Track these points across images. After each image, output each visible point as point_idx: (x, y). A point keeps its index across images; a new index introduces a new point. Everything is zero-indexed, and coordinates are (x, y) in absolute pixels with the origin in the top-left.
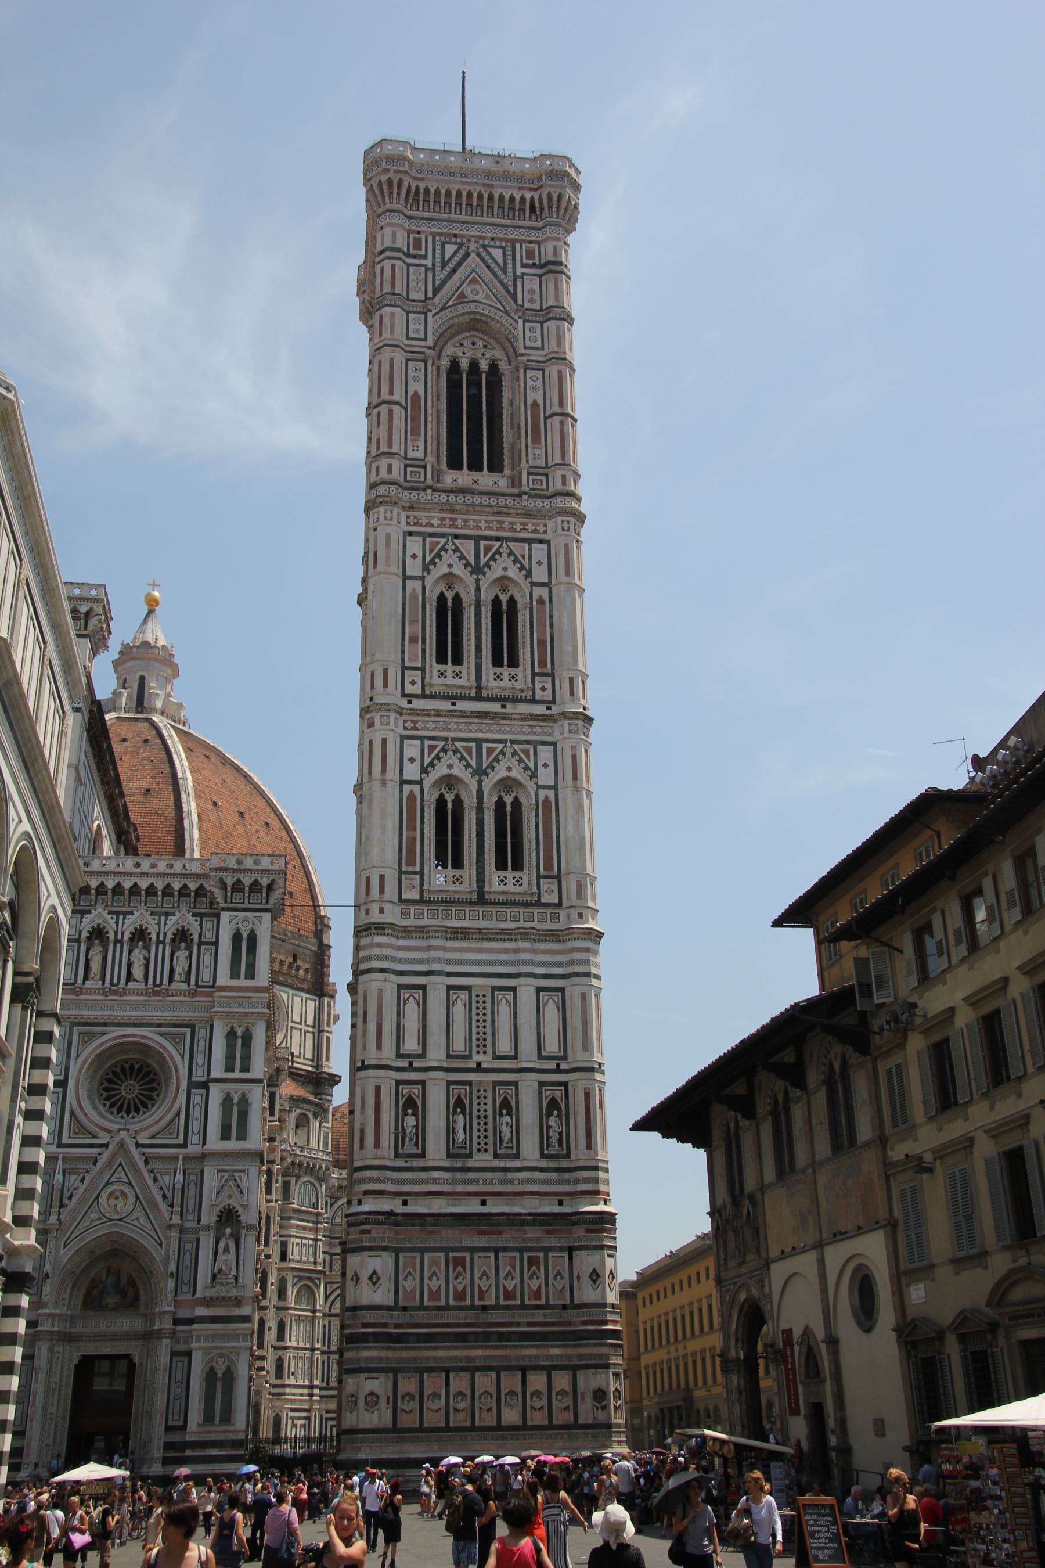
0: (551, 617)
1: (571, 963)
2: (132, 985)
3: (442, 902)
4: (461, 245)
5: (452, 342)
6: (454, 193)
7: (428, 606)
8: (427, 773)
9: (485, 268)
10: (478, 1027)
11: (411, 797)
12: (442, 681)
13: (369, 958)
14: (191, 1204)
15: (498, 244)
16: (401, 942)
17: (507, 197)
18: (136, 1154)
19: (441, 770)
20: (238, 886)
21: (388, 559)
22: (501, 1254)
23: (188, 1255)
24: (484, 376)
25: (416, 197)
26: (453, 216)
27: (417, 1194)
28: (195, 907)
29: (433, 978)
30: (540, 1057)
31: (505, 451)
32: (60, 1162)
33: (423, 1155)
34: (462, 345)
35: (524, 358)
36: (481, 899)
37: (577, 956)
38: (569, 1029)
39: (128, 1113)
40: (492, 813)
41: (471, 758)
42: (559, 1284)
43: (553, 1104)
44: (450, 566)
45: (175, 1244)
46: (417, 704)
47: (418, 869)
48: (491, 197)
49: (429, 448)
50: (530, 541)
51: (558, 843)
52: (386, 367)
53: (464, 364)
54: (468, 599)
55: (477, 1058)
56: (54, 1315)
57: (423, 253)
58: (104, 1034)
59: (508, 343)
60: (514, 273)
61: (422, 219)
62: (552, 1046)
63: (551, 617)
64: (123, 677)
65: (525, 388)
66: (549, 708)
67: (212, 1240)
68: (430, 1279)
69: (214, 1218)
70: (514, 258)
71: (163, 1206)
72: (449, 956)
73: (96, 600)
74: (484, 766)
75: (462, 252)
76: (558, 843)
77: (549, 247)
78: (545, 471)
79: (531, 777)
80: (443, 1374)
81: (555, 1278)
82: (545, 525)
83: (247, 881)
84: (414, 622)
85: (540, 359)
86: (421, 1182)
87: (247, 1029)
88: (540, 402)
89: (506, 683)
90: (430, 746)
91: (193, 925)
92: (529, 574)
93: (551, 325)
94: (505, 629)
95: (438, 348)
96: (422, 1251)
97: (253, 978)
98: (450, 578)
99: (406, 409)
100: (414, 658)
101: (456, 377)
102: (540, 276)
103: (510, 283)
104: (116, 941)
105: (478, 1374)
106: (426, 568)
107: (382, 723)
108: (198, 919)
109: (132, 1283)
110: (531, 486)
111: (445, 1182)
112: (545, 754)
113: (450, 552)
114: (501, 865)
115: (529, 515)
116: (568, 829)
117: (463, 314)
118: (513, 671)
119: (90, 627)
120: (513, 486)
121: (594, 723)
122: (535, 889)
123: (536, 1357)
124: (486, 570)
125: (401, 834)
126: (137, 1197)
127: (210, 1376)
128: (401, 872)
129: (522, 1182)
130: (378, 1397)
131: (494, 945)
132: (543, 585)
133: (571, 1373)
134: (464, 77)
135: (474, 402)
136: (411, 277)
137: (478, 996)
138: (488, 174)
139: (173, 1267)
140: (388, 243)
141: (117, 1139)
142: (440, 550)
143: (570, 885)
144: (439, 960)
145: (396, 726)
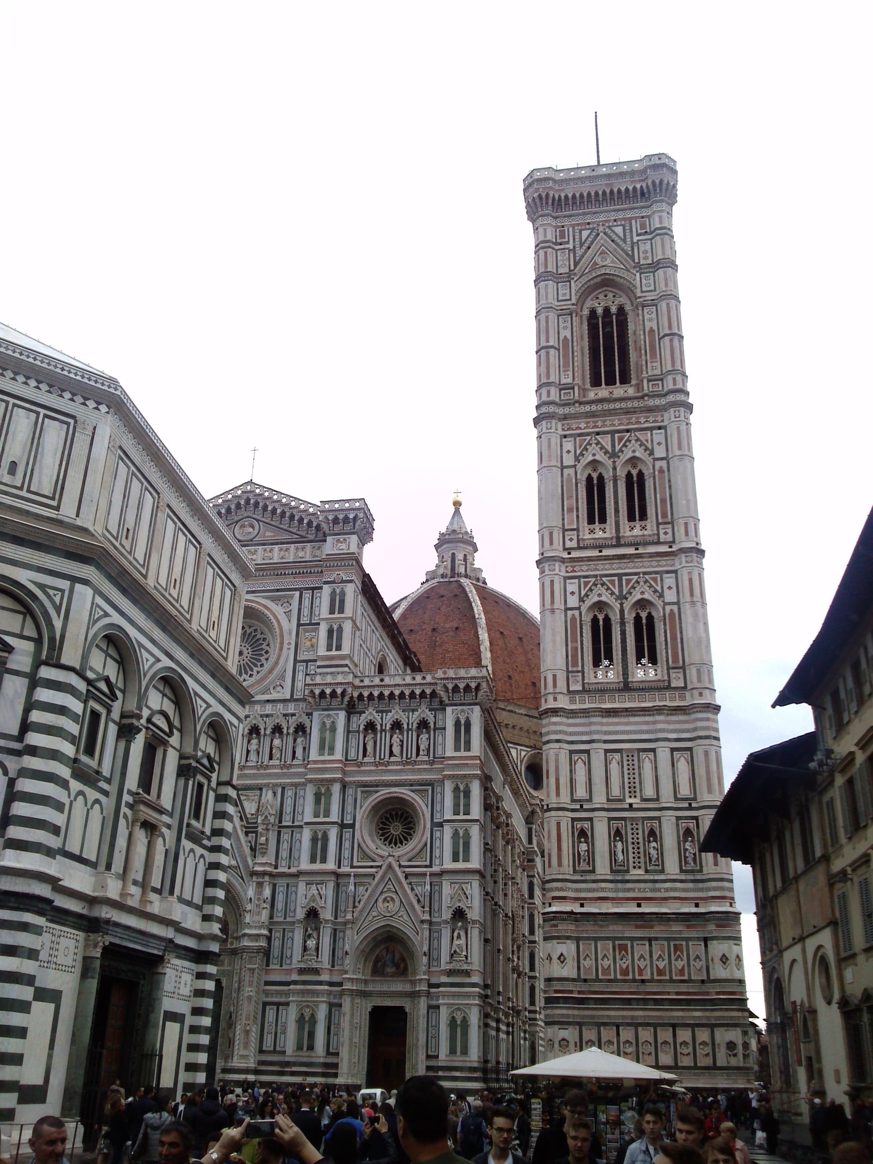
0: (669, 481)
1: (695, 729)
2: (393, 759)
5: (590, 298)
6: (585, 194)
8: (584, 601)
11: (573, 618)
13: (548, 733)
14: (436, 906)
15: (619, 223)
16: (571, 721)
17: (623, 189)
18: (399, 872)
20: (456, 689)
21: (550, 456)
22: (653, 943)
23: (436, 941)
24: (614, 317)
27: (590, 899)
29: (594, 745)
30: (676, 799)
31: (632, 368)
32: (352, 878)
33: (593, 871)
34: (597, 298)
36: (626, 687)
37: (699, 724)
39: (396, 844)
40: (632, 626)
41: (615, 588)
42: (698, 964)
43: (688, 832)
44: (594, 455)
45: (427, 933)
46: (575, 554)
47: (580, 669)
48: (612, 192)
49: (576, 374)
50: (651, 429)
52: (543, 323)
53: (600, 311)
54: (608, 475)
56: (353, 979)
58: (377, 792)
59: (629, 291)
60: (632, 241)
61: (565, 217)
62: (685, 790)
63: (669, 481)
66: (671, 547)
67: (449, 931)
68: (602, 959)
69: (450, 916)
71: (417, 907)
72: (605, 728)
73: (358, 509)
74: (624, 593)
76: (682, 643)
77: (656, 218)
79: (659, 597)
80: (615, 1028)
81: (695, 960)
82: (662, 416)
83: (462, 686)
86: (593, 890)
87: (467, 785)
88: (655, 328)
89: (637, 532)
90: (585, 582)
91: (430, 717)
92: (652, 453)
93: (661, 272)
95: (579, 304)
96: (596, 939)
97: (469, 750)
98: (594, 463)
99: (559, 350)
100: (572, 523)
101: (595, 321)
102: (651, 239)
104: (382, 730)
105: (640, 1029)
106: (577, 459)
107: (550, 570)
109: (403, 959)
111: (610, 890)
112: (669, 580)
113: (594, 445)
115: (650, 410)
116: (689, 632)
119: (357, 526)
120: (638, 392)
121: (706, 554)
122: (666, 678)
123: (682, 1017)
124: (620, 454)
126: (401, 901)
127: (453, 1023)
128: (568, 672)
129: (667, 890)
130: (568, 1042)
131: (637, 719)
132: (662, 459)
133: (709, 1030)
135: (608, 336)
138: (609, 176)
139: (426, 949)
140: (541, 238)
141: (387, 862)
143: (692, 673)
144: (597, 732)
145: (560, 571)
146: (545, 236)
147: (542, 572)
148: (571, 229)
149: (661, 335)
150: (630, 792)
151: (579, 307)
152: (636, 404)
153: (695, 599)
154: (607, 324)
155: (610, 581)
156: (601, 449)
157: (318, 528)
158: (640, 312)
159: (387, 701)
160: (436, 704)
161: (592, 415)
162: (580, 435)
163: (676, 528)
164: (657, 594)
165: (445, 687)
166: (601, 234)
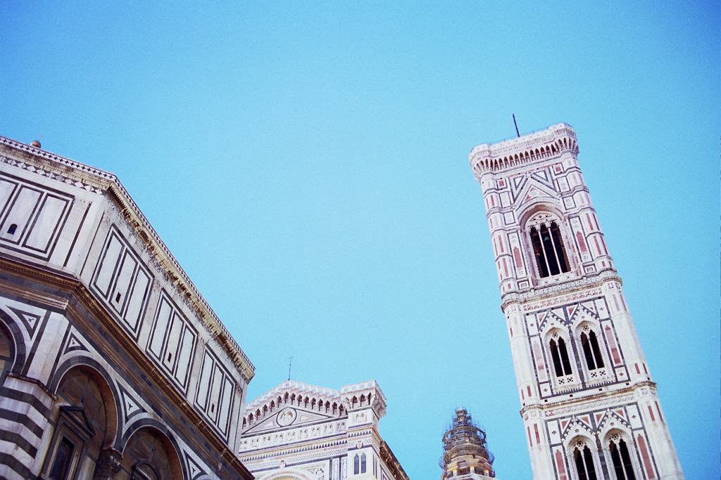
0: (616, 334)
4: (523, 177)
5: (529, 219)
7: (545, 348)
8: (564, 438)
11: (558, 453)
24: (549, 229)
25: (495, 165)
26: (516, 166)
35: (567, 214)
40: (609, 453)
46: (550, 401)
49: (528, 270)
50: (593, 300)
53: (538, 227)
63: (616, 334)
65: (571, 228)
70: (550, 173)
75: (524, 179)
78: (593, 263)
79: (627, 425)
84: (538, 359)
88: (581, 231)
92: (597, 316)
101: (535, 235)
106: (539, 329)
112: (632, 410)
113: (551, 317)
115: (590, 286)
119: (371, 403)
125: (556, 476)
132: (607, 319)
135: (548, 244)
145: (540, 416)
146: (489, 185)
148: (507, 179)
154: (545, 234)
155: (584, 419)
156: (557, 319)
157: (341, 408)
162: (538, 312)
164: (625, 423)
166: (530, 179)
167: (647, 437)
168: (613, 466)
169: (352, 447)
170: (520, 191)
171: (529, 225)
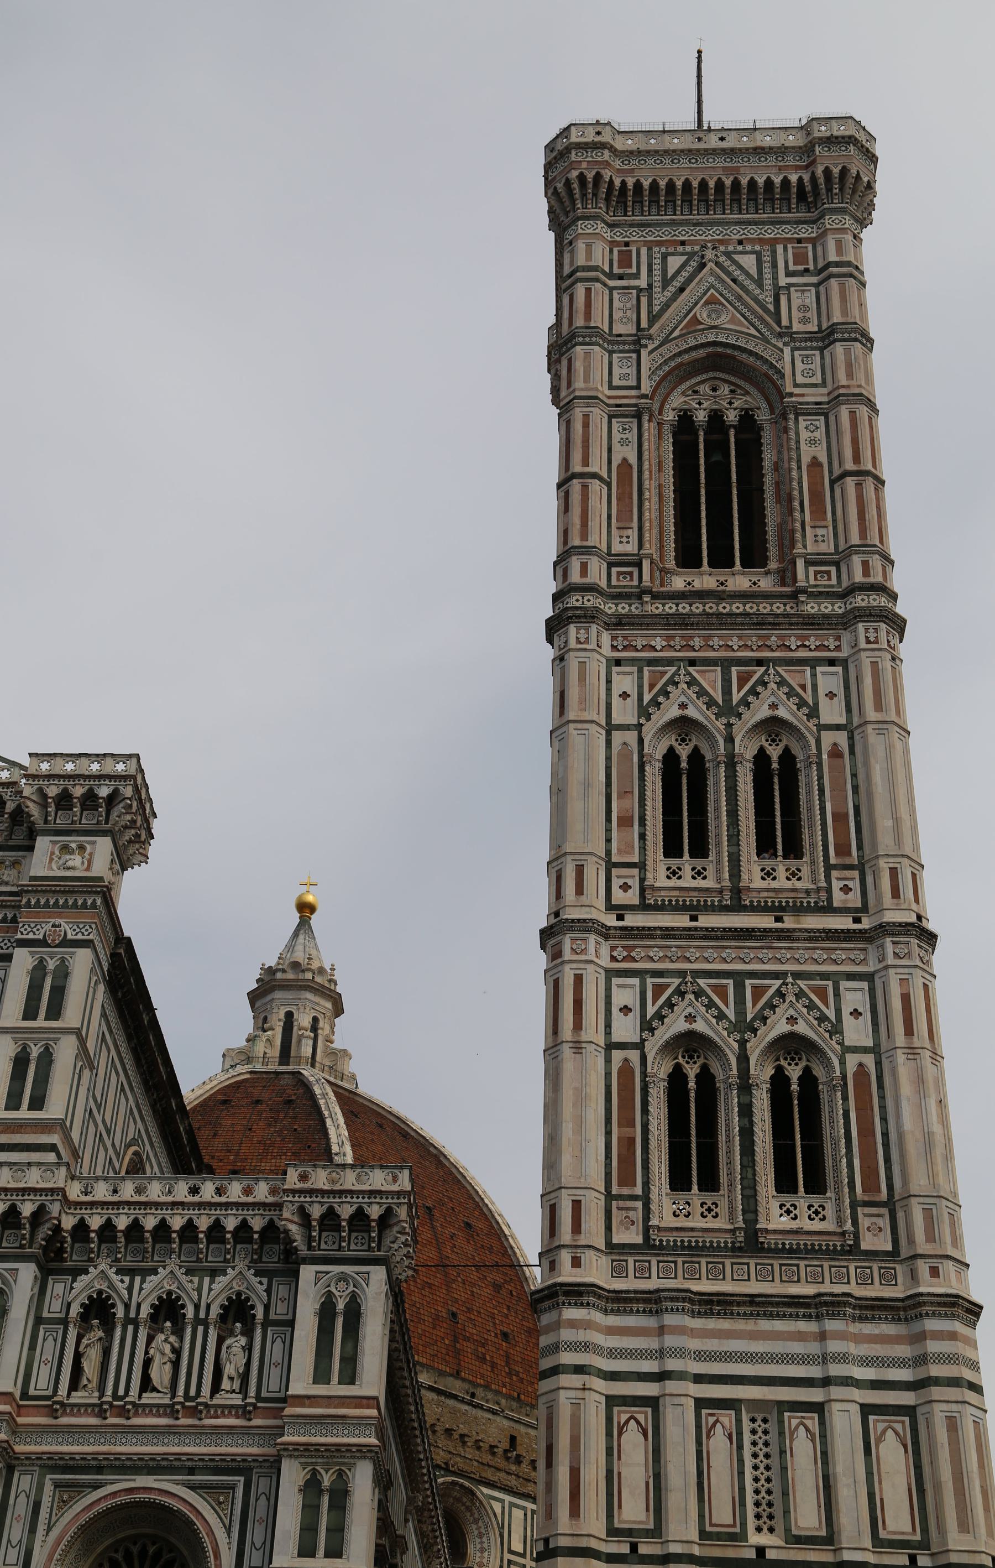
3: (683, 1247)
5: (679, 390)
6: (679, 184)
7: (647, 768)
8: (652, 1030)
9: (728, 281)
10: (756, 1480)
11: (626, 1069)
12: (673, 883)
15: (749, 248)
16: (613, 1320)
17: (761, 181)
19: (676, 1025)
21: (583, 701)
24: (732, 432)
28: (260, 1260)
34: (696, 392)
38: (928, 1486)
44: (683, 706)
46: (631, 920)
47: (638, 1190)
48: (736, 184)
51: (886, 1145)
53: (701, 416)
54: (715, 752)
55: (755, 1539)
57: (634, 270)
63: (854, 775)
64: (262, 1016)
65: (798, 442)
66: (857, 920)
70: (774, 265)
74: (749, 1019)
75: (694, 264)
76: (886, 1145)
79: (831, 1034)
82: (838, 638)
83: (346, 1211)
84: (625, 793)
85: (819, 399)
88: (823, 459)
89: (782, 882)
90: (655, 986)
92: (814, 712)
93: (839, 348)
94: (777, 800)
95: (658, 399)
99: (609, 485)
100: (628, 849)
102: (817, 285)
103: (770, 299)
106: (644, 712)
108: (265, 1280)
110: (812, 582)
114: (785, 1184)
115: (811, 622)
117: (696, 348)
118: (793, 864)
120: (783, 584)
122: (848, 1226)
128: (609, 1196)
131: (778, 1325)
132: (838, 727)
134: (699, 58)
135: (718, 472)
136: (616, 304)
137: (753, 1420)
142: (666, 684)
144: (680, 1353)
147: (555, 955)
149: (837, 472)
150: (758, 1517)
151: (656, 407)
152: (778, 608)
153: (917, 1043)
154: (717, 446)
155: (715, 988)
156: (699, 695)
158: (791, 424)
159: (149, 1246)
160: (272, 1260)
161: (682, 622)
162: (651, 662)
163: (869, 879)
165: (303, 1214)
167: (880, 1078)
168: (769, 1137)
169: (31, 936)
170: (674, 298)
171: (675, 405)
